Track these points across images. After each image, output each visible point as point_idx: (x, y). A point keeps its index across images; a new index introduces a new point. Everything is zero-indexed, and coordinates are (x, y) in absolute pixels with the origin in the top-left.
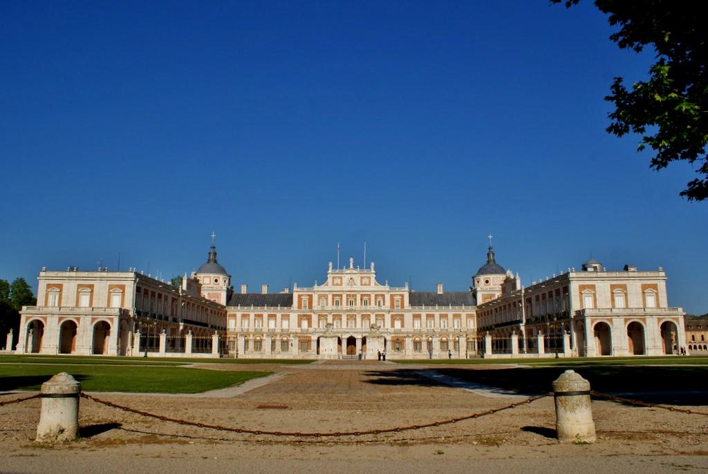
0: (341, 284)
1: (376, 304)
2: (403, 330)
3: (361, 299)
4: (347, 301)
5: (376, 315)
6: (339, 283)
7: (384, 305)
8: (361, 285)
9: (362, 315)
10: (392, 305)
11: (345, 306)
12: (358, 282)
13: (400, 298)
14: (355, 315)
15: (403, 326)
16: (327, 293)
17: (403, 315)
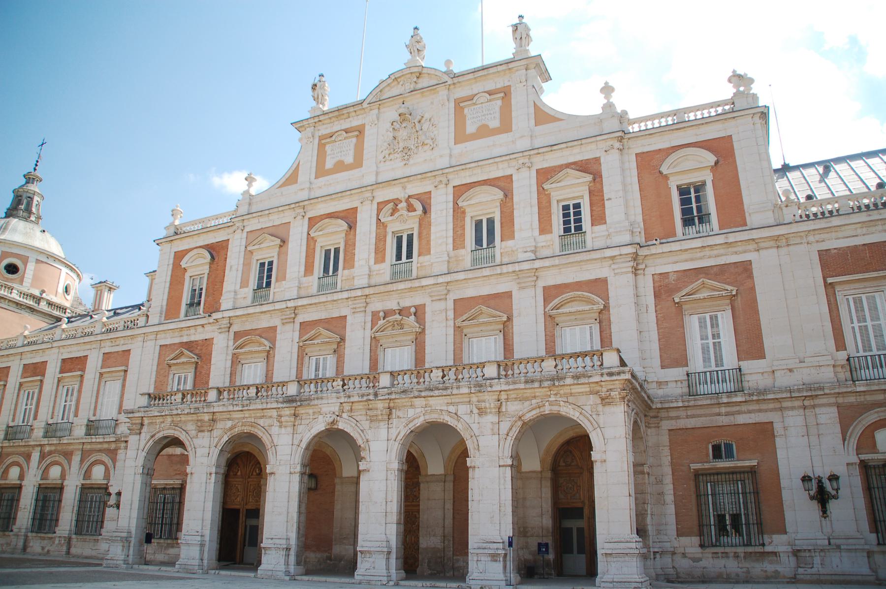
0: (358, 162)
1: (545, 227)
2: (755, 372)
3: (458, 213)
4: (380, 240)
5: (550, 293)
6: (349, 159)
7: (599, 218)
8: (461, 136)
9: (462, 306)
10: (656, 230)
11: (365, 266)
12: (445, 130)
13: (711, 159)
14: (419, 312)
15: (751, 344)
16: (287, 217)
17: (746, 268)
